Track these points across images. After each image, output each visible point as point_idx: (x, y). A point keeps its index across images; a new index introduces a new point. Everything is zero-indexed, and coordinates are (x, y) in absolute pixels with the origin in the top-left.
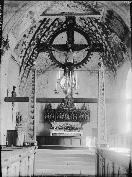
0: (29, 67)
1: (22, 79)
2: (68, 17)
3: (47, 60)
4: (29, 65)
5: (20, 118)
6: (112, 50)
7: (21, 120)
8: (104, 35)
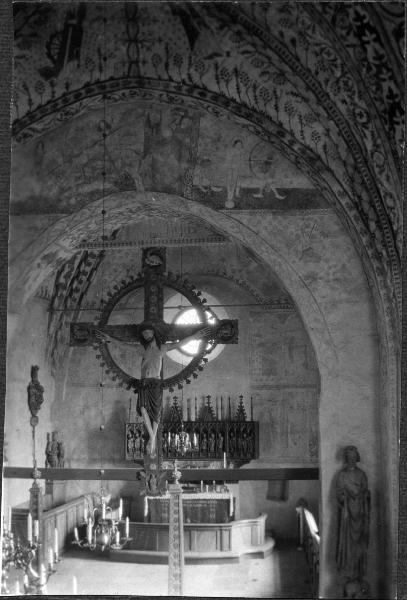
0: (77, 296)
1: (59, 333)
2: (148, 249)
3: (128, 271)
4: (77, 290)
5: (56, 451)
7: (59, 455)
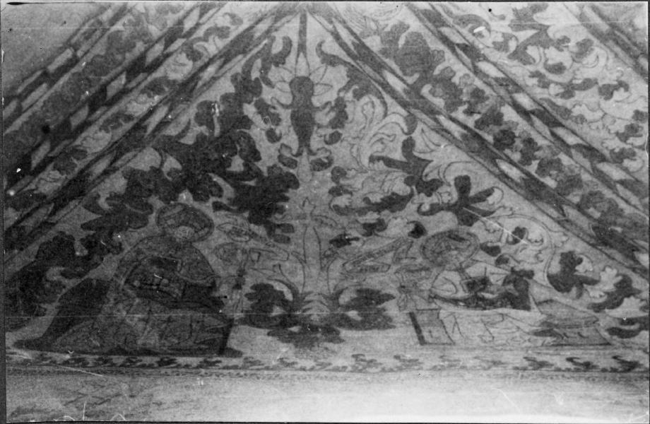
6: (80, 251)
8: (172, 163)
